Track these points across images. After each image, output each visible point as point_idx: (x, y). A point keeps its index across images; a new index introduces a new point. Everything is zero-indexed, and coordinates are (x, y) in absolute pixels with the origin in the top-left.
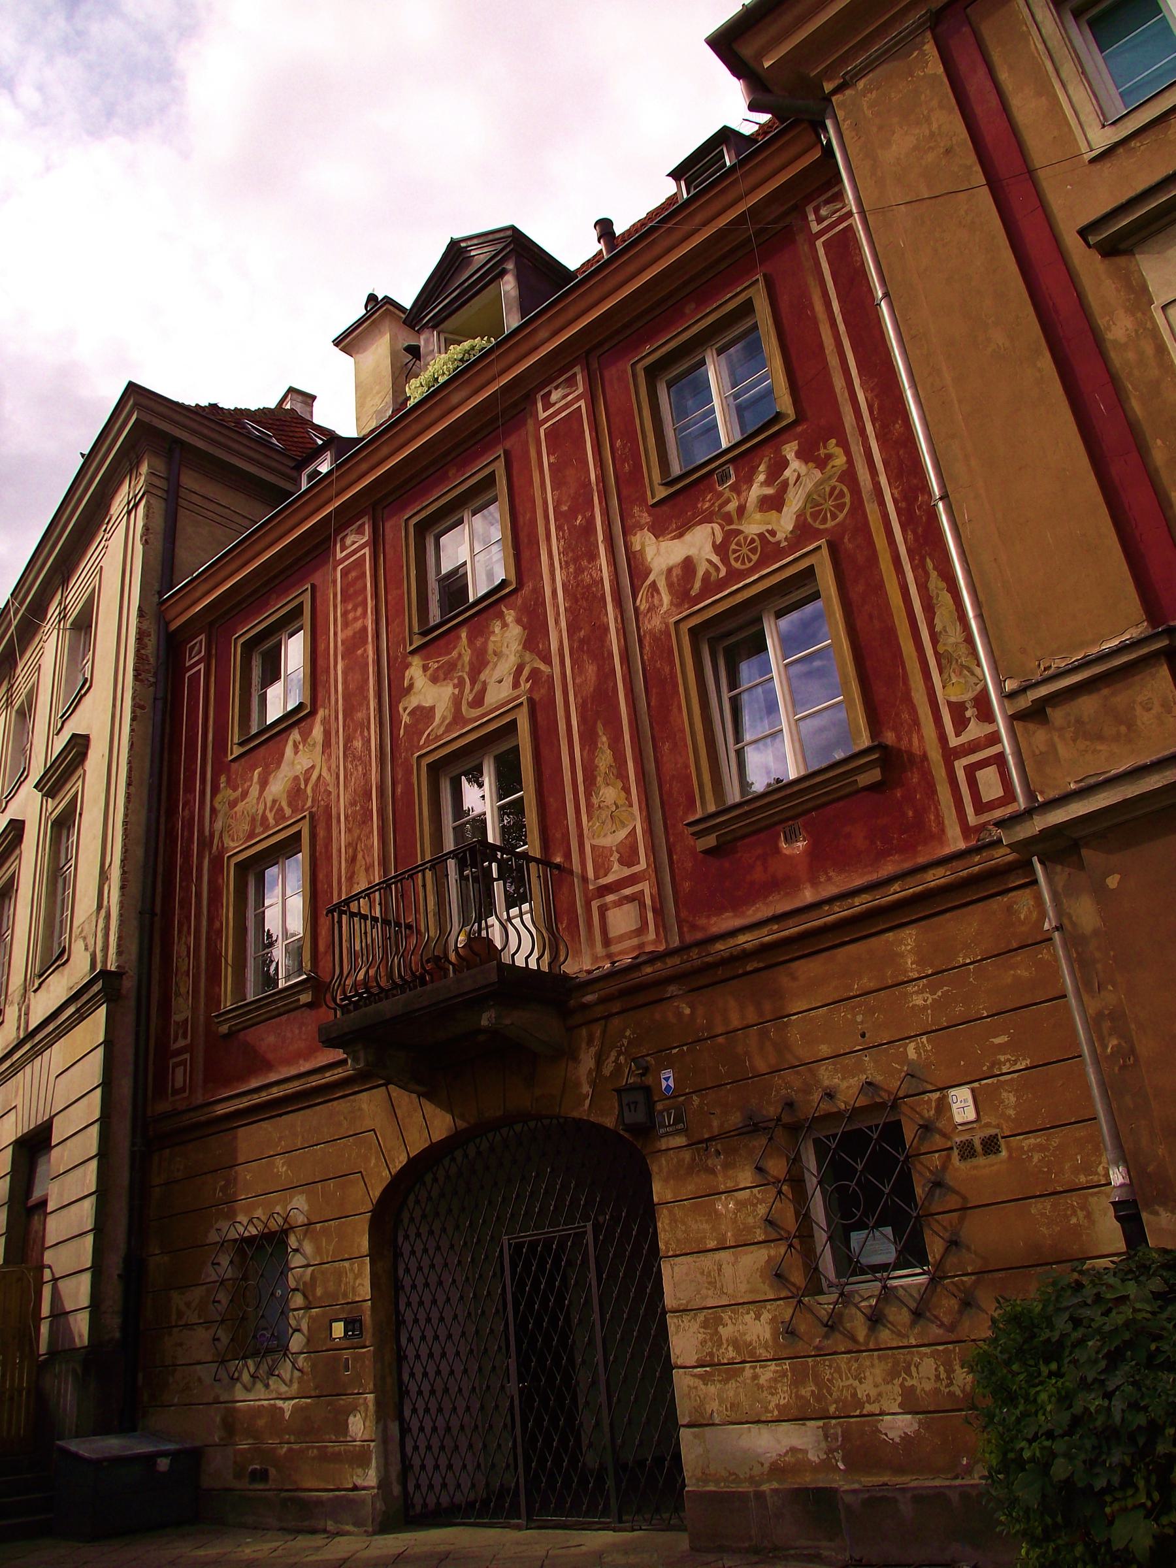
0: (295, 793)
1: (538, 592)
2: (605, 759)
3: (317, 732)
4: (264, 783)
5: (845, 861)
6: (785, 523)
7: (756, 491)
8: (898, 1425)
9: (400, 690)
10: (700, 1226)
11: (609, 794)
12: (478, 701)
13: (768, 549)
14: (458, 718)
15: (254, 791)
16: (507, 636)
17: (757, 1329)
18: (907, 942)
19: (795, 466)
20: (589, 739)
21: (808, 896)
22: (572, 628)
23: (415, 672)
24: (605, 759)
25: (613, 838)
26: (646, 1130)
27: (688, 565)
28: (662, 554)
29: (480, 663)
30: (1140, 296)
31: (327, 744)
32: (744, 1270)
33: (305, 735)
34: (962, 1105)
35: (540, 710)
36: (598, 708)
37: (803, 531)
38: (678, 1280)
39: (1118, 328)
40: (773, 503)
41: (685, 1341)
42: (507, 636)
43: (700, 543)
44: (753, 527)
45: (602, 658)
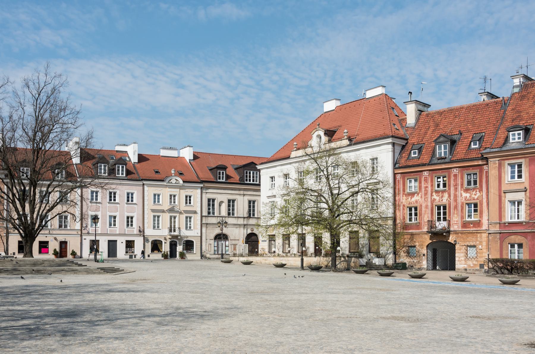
0: (416, 202)
1: (450, 192)
2: (456, 212)
3: (420, 195)
4: (411, 199)
5: (475, 227)
6: (476, 197)
7: (474, 193)
8: (472, 265)
9: (432, 195)
10: (459, 251)
11: (456, 215)
12: (442, 200)
13: (474, 199)
14: (439, 201)
15: (410, 199)
16: (446, 195)
17: (463, 259)
18: (479, 235)
19: (478, 192)
20: (454, 209)
21: (472, 229)
22: (454, 198)
23: (434, 194)
24: (456, 212)
25: (456, 220)
26: (456, 244)
27: (466, 197)
28: (464, 195)
29: (442, 197)
30: (505, 197)
31: (421, 197)
32: (463, 255)
33: (418, 195)
34: (480, 247)
35: (450, 205)
36: (456, 207)
37: (477, 199)
38: (457, 255)
39: (503, 198)
40: (475, 195)
41: (457, 259)
42: (446, 195)
43: (468, 195)
44: (473, 196)
45: (457, 202)
